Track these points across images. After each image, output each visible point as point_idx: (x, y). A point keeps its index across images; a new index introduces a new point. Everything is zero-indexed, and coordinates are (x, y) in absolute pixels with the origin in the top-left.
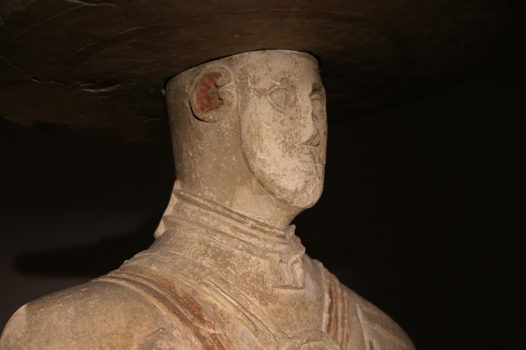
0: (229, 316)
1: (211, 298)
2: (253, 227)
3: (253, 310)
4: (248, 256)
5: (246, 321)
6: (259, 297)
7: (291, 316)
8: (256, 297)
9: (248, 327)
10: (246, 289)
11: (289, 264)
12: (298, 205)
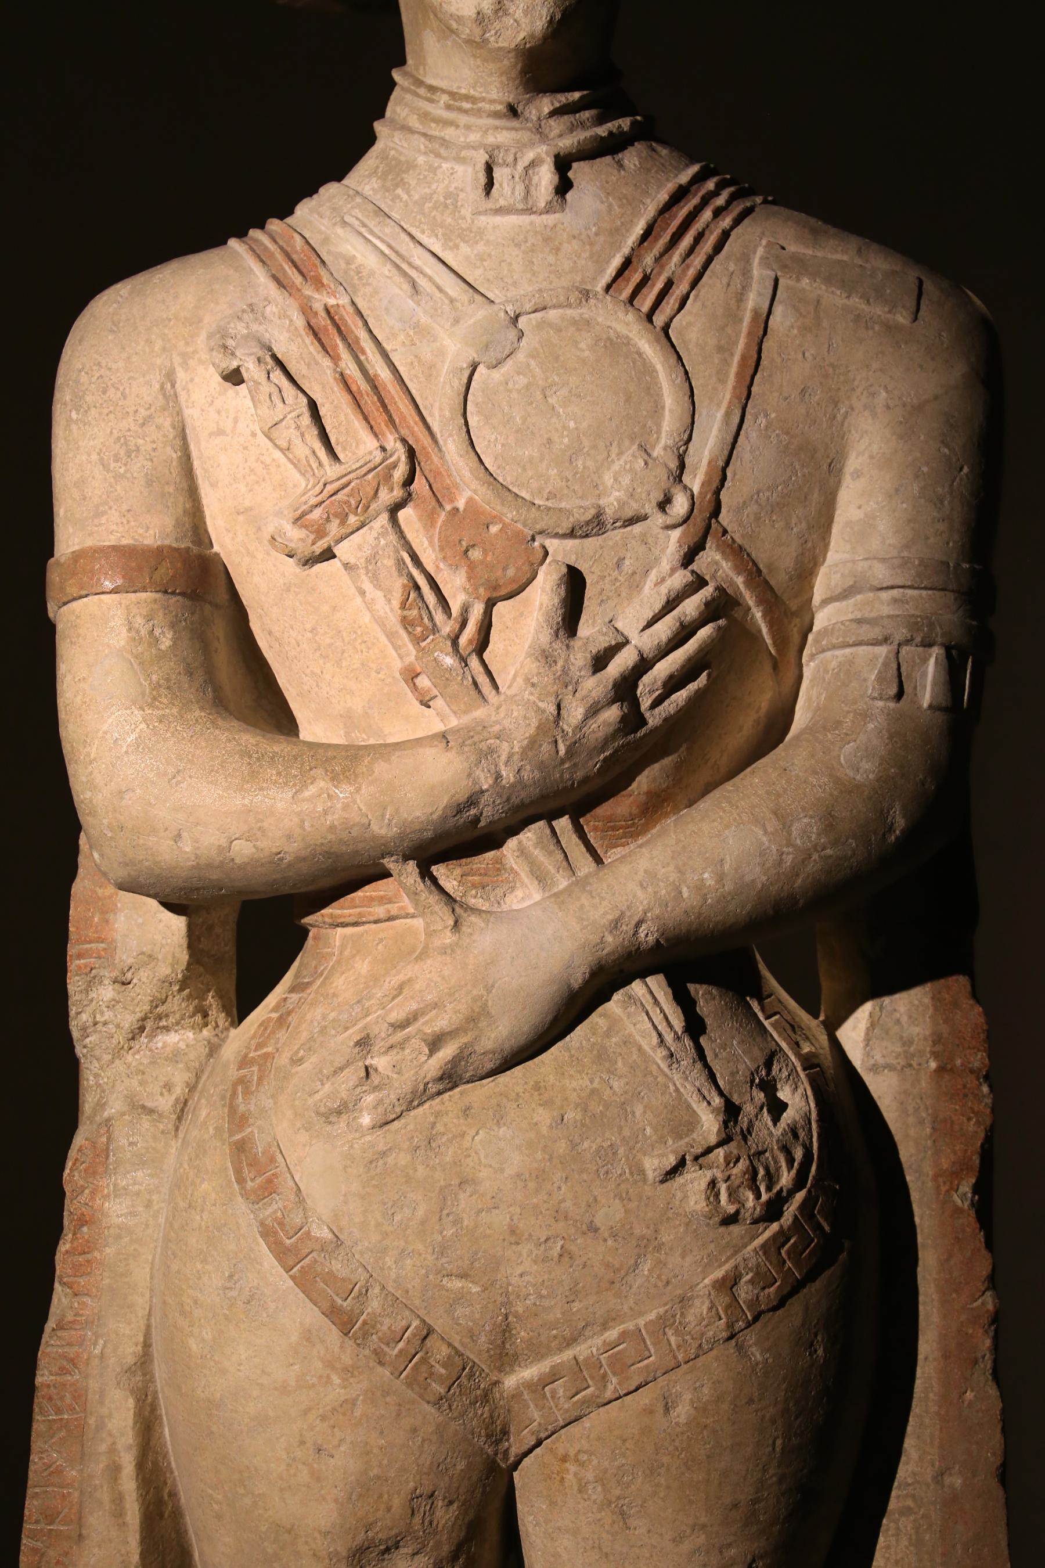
0: (372, 274)
1: (349, 247)
2: (448, 107)
3: (419, 258)
4: (436, 162)
5: (398, 278)
6: (443, 235)
7: (510, 264)
8: (437, 236)
10: (421, 223)
11: (520, 166)
12: (500, 45)
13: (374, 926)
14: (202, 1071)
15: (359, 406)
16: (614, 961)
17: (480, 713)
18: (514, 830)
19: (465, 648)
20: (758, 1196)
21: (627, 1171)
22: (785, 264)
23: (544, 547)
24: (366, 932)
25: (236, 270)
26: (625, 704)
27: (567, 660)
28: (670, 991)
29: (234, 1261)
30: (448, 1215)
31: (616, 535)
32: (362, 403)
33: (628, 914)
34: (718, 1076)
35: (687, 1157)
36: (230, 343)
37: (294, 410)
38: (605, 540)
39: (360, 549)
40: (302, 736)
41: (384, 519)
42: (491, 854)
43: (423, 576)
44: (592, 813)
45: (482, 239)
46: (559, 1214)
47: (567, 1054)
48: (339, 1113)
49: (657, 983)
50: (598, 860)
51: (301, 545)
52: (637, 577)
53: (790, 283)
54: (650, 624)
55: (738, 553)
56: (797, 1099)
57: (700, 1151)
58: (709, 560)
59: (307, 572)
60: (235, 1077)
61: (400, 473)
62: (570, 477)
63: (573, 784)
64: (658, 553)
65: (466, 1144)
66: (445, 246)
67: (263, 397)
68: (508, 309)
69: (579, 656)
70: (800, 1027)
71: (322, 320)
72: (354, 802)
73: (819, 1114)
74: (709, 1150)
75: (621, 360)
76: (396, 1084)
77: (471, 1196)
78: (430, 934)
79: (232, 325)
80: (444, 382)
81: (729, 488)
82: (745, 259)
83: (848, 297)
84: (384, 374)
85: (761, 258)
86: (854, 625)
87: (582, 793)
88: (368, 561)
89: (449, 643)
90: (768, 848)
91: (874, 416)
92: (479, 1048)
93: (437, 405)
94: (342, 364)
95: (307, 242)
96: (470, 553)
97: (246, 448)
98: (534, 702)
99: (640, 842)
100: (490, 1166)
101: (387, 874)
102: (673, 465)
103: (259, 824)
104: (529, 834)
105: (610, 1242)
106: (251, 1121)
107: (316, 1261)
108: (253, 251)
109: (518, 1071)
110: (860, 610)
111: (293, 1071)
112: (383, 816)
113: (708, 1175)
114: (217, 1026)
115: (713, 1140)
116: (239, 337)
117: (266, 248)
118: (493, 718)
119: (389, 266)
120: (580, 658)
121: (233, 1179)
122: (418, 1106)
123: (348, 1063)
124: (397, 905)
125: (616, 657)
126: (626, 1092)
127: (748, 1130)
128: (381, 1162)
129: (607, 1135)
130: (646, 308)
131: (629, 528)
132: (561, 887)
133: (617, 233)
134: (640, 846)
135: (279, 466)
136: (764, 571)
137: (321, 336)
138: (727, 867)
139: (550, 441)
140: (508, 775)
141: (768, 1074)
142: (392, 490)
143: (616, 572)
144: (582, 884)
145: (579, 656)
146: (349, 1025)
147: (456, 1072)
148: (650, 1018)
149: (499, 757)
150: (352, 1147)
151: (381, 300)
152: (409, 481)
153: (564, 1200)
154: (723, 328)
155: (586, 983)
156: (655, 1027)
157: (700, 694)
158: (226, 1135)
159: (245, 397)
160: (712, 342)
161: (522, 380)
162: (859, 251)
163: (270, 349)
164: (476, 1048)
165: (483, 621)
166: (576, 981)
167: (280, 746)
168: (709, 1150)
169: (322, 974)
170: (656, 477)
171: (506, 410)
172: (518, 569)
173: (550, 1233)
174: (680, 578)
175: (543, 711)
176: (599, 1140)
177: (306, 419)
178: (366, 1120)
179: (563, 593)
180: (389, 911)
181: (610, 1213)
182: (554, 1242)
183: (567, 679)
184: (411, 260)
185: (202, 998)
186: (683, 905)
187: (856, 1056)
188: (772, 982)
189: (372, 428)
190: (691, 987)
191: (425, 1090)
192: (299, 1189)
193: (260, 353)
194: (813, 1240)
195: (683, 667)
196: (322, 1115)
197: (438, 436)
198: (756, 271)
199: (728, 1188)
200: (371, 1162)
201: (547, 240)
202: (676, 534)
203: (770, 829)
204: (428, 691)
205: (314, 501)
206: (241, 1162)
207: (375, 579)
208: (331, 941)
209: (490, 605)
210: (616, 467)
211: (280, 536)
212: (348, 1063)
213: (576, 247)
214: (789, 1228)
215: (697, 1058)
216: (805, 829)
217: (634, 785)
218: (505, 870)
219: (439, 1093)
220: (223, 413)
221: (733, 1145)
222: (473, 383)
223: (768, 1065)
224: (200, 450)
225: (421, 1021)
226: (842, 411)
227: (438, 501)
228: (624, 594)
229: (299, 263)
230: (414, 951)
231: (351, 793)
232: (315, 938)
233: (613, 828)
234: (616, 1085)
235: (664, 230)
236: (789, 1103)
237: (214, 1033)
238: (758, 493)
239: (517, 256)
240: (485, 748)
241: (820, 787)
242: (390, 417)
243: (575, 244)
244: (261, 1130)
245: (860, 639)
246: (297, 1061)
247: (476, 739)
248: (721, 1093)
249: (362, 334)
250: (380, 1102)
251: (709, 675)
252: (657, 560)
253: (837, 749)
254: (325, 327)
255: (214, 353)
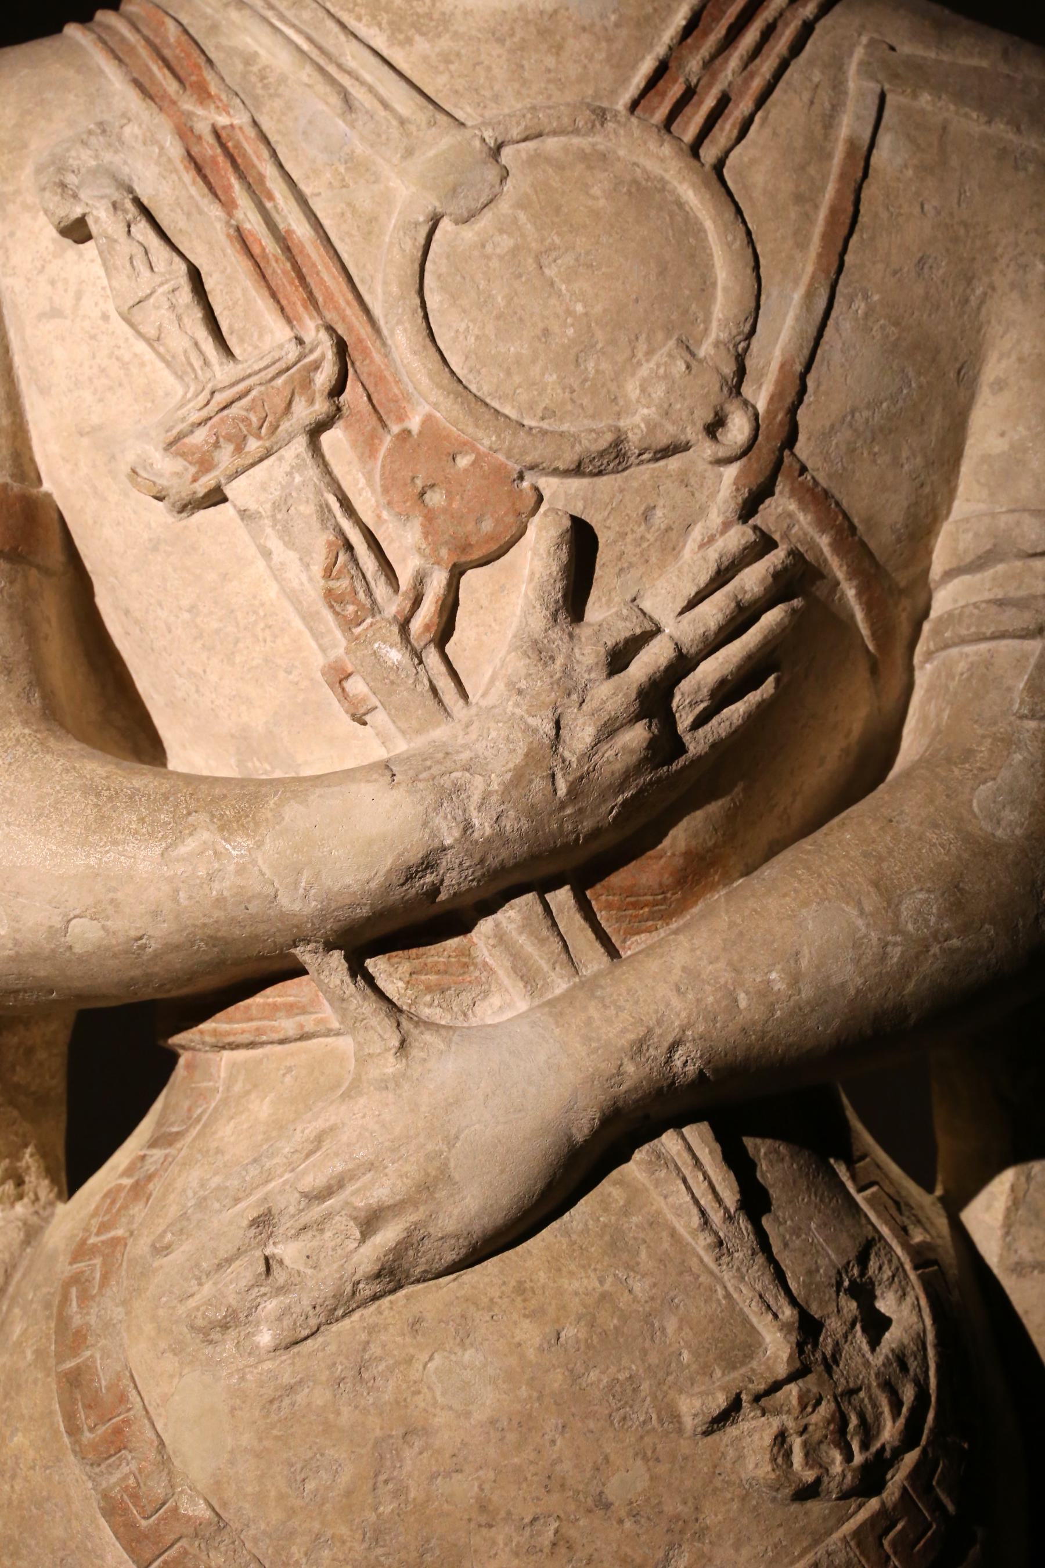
0: (283, 79)
1: (249, 40)
3: (353, 57)
6: (391, 23)
7: (489, 69)
8: (379, 25)
9: (327, 103)
13: (278, 1048)
14: (14, 1267)
15: (264, 277)
16: (636, 1101)
17: (440, 733)
18: (489, 907)
19: (419, 638)
20: (849, 1457)
21: (654, 1416)
22: (892, 71)
23: (537, 489)
24: (267, 1056)
25: (79, 71)
26: (655, 721)
27: (569, 657)
28: (717, 1147)
29: (61, 1554)
30: (386, 1482)
31: (642, 473)
32: (268, 273)
33: (658, 1031)
34: (789, 1275)
35: (744, 1397)
36: (71, 179)
37: (167, 281)
38: (627, 480)
39: (265, 490)
40: (173, 764)
41: (300, 444)
42: (453, 943)
43: (357, 530)
44: (605, 883)
45: (447, 30)
46: (552, 1482)
47: (565, 1241)
48: (225, 1327)
49: (698, 1134)
50: (613, 952)
51: (175, 481)
52: (673, 535)
53: (904, 100)
54: (692, 604)
55: (821, 501)
56: (905, 1312)
57: (762, 1387)
58: (780, 510)
59: (184, 523)
60: (66, 1274)
61: (324, 377)
62: (575, 387)
63: (577, 838)
64: (704, 499)
65: (414, 1375)
66: (392, 40)
67: (120, 261)
68: (486, 135)
69: (588, 650)
70: (908, 1205)
71: (209, 148)
72: (254, 862)
73: (939, 1335)
74: (776, 1387)
75: (653, 213)
76: (311, 1284)
77: (421, 1453)
78: (363, 1060)
79: (73, 153)
80: (391, 244)
81: (809, 405)
82: (836, 66)
83: (989, 122)
84: (301, 230)
85: (861, 63)
86: (994, 609)
87: (593, 852)
88: (276, 507)
89: (395, 629)
90: (865, 936)
91: (1025, 298)
92: (435, 1231)
93: (380, 277)
94: (239, 214)
95: (186, 32)
96: (427, 496)
97: (93, 337)
98: (521, 718)
99: (674, 926)
100: (451, 1408)
101: (299, 971)
102: (729, 369)
103: (111, 895)
104: (512, 913)
105: (628, 1525)
106: (91, 1340)
107: (186, 1553)
108: (105, 43)
109: (492, 1265)
110: (1001, 586)
111: (156, 1264)
112: (296, 883)
113: (775, 1423)
114: (37, 1198)
115: (782, 1370)
116: (83, 170)
117: (123, 39)
118: (461, 741)
119: (309, 69)
120: (589, 654)
121: (62, 1429)
122: (343, 1316)
123: (239, 1253)
124: (314, 1016)
125: (642, 653)
126: (652, 1299)
127: (833, 1356)
128: (286, 1401)
129: (625, 1362)
130: (689, 135)
131: (662, 463)
132: (558, 992)
133: (645, 25)
134: (676, 932)
135: (142, 364)
136: (860, 527)
137: (207, 171)
138: (804, 963)
139: (546, 332)
140: (483, 825)
141: (863, 1272)
142: (311, 402)
143: (643, 527)
144: (589, 986)
145: (588, 650)
146: (241, 1195)
147: (400, 1266)
148: (689, 1188)
149: (469, 797)
150: (243, 1378)
151: (296, 119)
152: (338, 389)
153: (559, 1460)
154: (802, 168)
155: (596, 1134)
156: (696, 1202)
157: (763, 710)
158: (52, 1362)
159: (92, 261)
160: (787, 187)
161: (506, 242)
162: (1005, 54)
163: (130, 190)
164: (431, 1230)
165: (446, 597)
166: (580, 1130)
167: (142, 779)
168: (776, 1387)
169: (198, 1119)
170: (703, 387)
171: (483, 284)
172: (497, 522)
173: (538, 1510)
174: (738, 537)
175: (535, 731)
176: (613, 1369)
177: (185, 295)
178: (265, 1338)
179: (564, 556)
180: (302, 1026)
181: (628, 1481)
182: (546, 1524)
183: (570, 684)
184: (342, 60)
185: (15, 1155)
186: (739, 1019)
187: (991, 1250)
188: (865, 1139)
189: (282, 309)
190: (749, 1142)
191: (354, 1293)
192: (162, 1443)
193: (116, 196)
194: (930, 1527)
195: (740, 667)
196: (200, 1330)
197: (382, 323)
198: (853, 83)
199: (805, 1444)
200: (271, 1402)
201: (543, 33)
202: (731, 472)
203: (868, 908)
204: (364, 700)
205: (196, 417)
206: (74, 1402)
207: (286, 533)
208: (213, 1070)
209: (457, 573)
210: (644, 371)
211: (145, 469)
212: (239, 1253)
213: (587, 44)
214: (895, 1507)
215: (757, 1248)
216: (920, 907)
217: (666, 842)
218: (475, 965)
219: (375, 1298)
220: (60, 285)
221: (811, 1378)
222: (433, 245)
223: (863, 1259)
224: (23, 339)
225: (350, 1188)
226: (979, 291)
227: (380, 419)
228: (653, 560)
229: (174, 63)
230: (338, 1085)
231: (249, 850)
232: (189, 1066)
233: (635, 905)
234: (638, 1287)
235: (717, 20)
236: (894, 1317)
237: (32, 1210)
238: (853, 413)
239: (499, 56)
240: (448, 785)
241: (943, 846)
242: (311, 294)
243: (586, 40)
244: (106, 1354)
245: (1003, 629)
246: (161, 1250)
247: (435, 771)
248: (793, 1301)
249: (269, 170)
250: (286, 1311)
251: (778, 681)
252: (703, 511)
253: (967, 790)
254: (213, 159)
255: (47, 194)
